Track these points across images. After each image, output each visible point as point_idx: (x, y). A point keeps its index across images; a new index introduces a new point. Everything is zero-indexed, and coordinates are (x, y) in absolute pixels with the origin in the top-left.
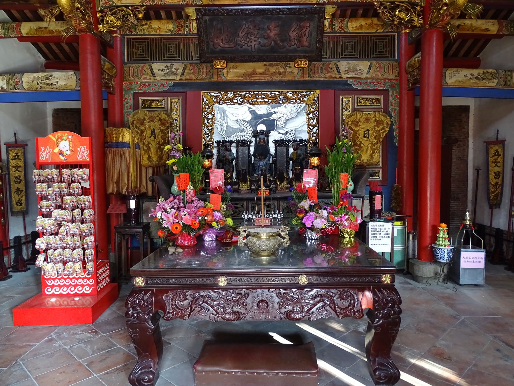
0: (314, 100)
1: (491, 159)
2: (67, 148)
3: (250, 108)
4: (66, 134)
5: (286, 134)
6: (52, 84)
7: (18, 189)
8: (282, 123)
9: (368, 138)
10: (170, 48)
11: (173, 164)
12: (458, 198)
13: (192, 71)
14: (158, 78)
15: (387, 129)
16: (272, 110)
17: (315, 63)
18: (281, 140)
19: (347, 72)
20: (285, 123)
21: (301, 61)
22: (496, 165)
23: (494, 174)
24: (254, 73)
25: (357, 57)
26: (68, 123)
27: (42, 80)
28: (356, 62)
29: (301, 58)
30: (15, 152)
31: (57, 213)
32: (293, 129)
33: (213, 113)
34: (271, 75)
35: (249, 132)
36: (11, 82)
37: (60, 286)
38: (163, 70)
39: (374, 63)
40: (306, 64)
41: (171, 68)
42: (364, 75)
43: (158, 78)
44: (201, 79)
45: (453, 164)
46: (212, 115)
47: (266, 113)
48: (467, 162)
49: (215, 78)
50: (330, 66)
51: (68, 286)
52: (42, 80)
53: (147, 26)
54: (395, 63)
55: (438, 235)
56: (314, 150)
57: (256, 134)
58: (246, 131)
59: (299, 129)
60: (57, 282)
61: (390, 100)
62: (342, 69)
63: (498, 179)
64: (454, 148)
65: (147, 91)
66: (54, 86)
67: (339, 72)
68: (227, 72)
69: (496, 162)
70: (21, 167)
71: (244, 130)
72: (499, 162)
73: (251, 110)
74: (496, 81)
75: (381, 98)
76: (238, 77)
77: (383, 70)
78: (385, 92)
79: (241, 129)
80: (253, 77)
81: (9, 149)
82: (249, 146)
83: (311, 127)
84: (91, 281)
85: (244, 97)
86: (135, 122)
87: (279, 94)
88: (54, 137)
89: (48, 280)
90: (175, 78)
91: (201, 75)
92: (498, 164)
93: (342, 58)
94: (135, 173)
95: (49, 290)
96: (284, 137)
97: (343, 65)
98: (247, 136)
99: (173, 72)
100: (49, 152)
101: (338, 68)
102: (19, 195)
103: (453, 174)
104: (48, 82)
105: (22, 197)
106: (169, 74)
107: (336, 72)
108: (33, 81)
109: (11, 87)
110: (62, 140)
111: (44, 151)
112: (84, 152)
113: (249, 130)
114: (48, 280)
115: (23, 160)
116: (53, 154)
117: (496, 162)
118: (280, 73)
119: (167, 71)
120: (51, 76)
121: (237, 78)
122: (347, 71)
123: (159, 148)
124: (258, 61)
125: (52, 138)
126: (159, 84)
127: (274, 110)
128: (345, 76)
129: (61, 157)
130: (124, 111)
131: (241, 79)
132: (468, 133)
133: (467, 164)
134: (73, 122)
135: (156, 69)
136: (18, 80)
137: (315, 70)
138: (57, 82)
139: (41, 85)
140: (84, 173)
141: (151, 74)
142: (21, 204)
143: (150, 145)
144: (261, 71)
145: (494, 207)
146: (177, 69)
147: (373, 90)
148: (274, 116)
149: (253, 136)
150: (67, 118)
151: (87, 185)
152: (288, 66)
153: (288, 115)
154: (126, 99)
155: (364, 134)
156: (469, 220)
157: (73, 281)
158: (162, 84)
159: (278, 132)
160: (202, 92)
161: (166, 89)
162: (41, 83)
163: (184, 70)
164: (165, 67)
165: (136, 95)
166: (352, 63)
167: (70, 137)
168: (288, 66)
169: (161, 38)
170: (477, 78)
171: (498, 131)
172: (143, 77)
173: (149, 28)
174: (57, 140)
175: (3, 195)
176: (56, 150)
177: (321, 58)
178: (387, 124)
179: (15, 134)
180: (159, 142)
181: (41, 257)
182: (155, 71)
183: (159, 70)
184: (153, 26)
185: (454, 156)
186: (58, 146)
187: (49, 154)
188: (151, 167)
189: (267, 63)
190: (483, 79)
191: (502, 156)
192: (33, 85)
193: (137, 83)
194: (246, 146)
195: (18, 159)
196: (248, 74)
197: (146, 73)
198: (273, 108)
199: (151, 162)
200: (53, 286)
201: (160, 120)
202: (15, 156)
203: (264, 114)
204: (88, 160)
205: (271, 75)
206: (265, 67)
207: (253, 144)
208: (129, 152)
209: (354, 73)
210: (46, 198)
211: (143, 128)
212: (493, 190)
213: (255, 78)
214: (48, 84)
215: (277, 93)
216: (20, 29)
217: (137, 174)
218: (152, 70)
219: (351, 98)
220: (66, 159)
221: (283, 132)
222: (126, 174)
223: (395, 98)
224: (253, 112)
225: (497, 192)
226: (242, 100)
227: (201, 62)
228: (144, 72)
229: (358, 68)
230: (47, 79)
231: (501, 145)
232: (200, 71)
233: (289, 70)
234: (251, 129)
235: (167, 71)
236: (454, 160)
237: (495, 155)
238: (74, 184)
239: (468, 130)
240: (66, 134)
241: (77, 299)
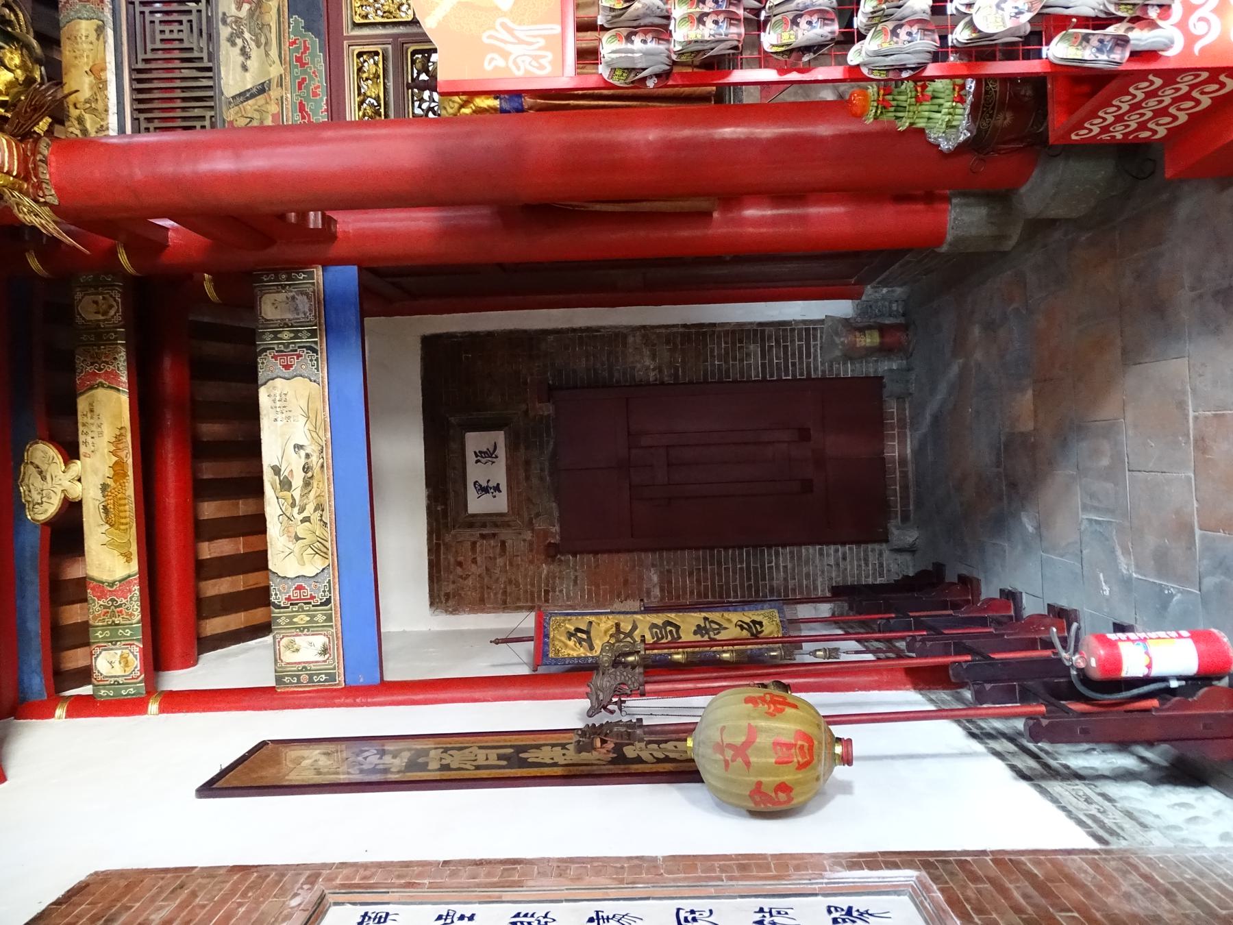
6: (306, 469)
7: (699, 630)
10: (167, 36)
14: (275, 70)
26: (474, 561)
27: (293, 505)
30: (563, 639)
36: (302, 619)
38: (244, 52)
41: (238, 20)
52: (293, 505)
53: (87, 116)
66: (314, 459)
70: (618, 625)
81: (551, 655)
100: (510, 31)
102: (721, 628)
104: (297, 481)
105: (729, 621)
106: (260, 28)
108: (297, 538)
109: (320, 618)
111: (505, 55)
115: (592, 618)
119: (247, 35)
120: (276, 470)
134: (474, 543)
135: (244, 80)
136: (294, 595)
138: (298, 447)
139: (310, 508)
141: (260, 99)
142: (760, 623)
150: (460, 564)
158: (299, 59)
161: (313, 41)
162: (302, 510)
164: (234, 44)
169: (132, 70)
173: (93, 111)
175: (724, 652)
179: (497, 642)
182: (249, 82)
183: (245, 68)
184: (86, 93)
187: (522, 31)
192: (310, 538)
195: (587, 632)
197: (256, 116)
202: (580, 641)
214: (307, 484)
216: (112, 584)
218: (245, 96)
230: (286, 485)
235: (247, 35)
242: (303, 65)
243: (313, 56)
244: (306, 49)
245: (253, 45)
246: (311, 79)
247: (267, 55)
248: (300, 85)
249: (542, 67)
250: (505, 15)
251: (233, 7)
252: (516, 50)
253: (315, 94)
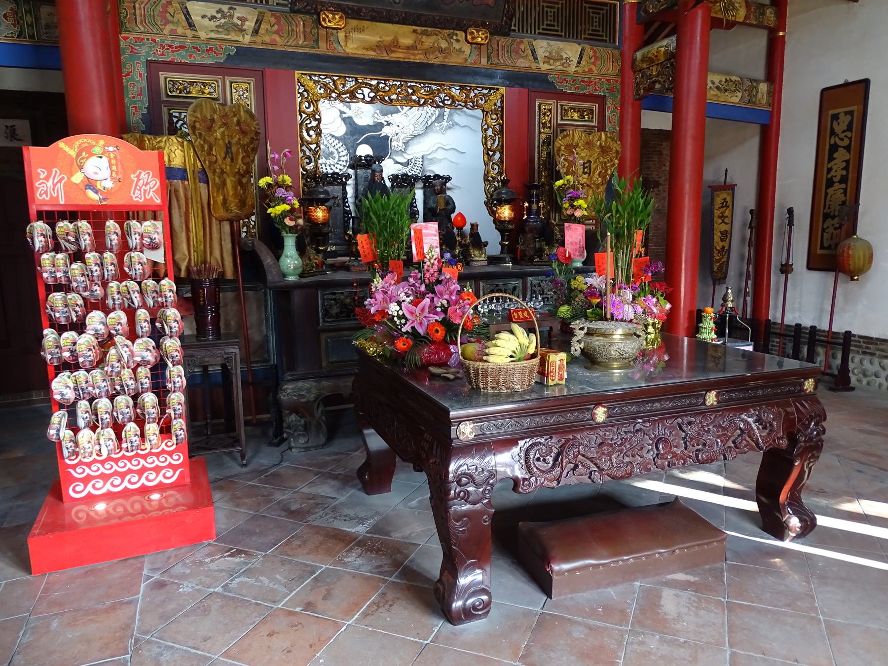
0: (495, 105)
2: (105, 173)
3: (342, 112)
4: (102, 142)
5: (407, 164)
8: (401, 144)
9: (589, 174)
11: (284, 214)
13: (276, 27)
15: (617, 161)
16: (383, 119)
17: (498, 38)
18: (403, 175)
19: (547, 60)
20: (406, 144)
21: (478, 32)
22: (723, 222)
23: (719, 235)
24: (394, 45)
25: (561, 36)
28: (560, 44)
29: (479, 26)
31: (95, 319)
32: (420, 155)
33: (317, 117)
34: (426, 52)
35: (342, 159)
37: (105, 477)
38: (213, 18)
39: (588, 48)
40: (486, 37)
41: (231, 16)
42: (573, 69)
43: (203, 35)
44: (296, 46)
46: (316, 120)
47: (371, 123)
49: (323, 49)
50: (522, 47)
51: (123, 475)
54: (616, 52)
55: (701, 325)
56: (504, 193)
57: (356, 163)
58: (337, 157)
59: (429, 157)
60: (97, 469)
61: (608, 114)
62: (541, 53)
65: (177, 59)
67: (535, 59)
68: (346, 36)
69: (723, 216)
71: (332, 153)
73: (344, 115)
74: (739, 94)
75: (595, 107)
76: (367, 49)
77: (599, 62)
78: (601, 100)
79: (327, 151)
80: (392, 52)
82: (344, 185)
83: (491, 153)
84: (176, 458)
85: (375, 89)
86: (197, 125)
87: (438, 90)
88: (71, 147)
89: (74, 467)
90: (240, 39)
91: (291, 38)
92: (726, 220)
93: (539, 33)
94: (201, 234)
95: (78, 489)
96: (405, 170)
97: (543, 46)
98: (338, 166)
99: (236, 25)
100: (60, 181)
101: (534, 52)
107: (531, 58)
110: (91, 155)
111: (47, 178)
112: (147, 184)
113: (342, 154)
114: (74, 467)
116: (69, 186)
118: (441, 51)
121: (365, 52)
122: (548, 58)
123: (240, 183)
124: (403, 22)
125: (67, 149)
126: (204, 47)
127: (386, 118)
128: (544, 67)
129: (91, 194)
130: (127, 101)
131: (372, 54)
135: (196, 15)
137: (498, 50)
140: (153, 229)
141: (185, 24)
143: (225, 175)
144: (407, 41)
146: (243, 20)
147: (584, 95)
148: (386, 131)
149: (351, 167)
151: (158, 256)
152: (455, 37)
153: (410, 130)
154: (128, 74)
155: (584, 169)
156: (732, 301)
157: (162, 459)
158: (211, 49)
159: (394, 160)
160: (297, 74)
161: (221, 59)
163: (259, 22)
164: (218, 12)
165: (153, 67)
166: (556, 45)
167: (111, 149)
168: (455, 37)
170: (718, 88)
171: (726, 171)
172: (169, 27)
174: (79, 154)
176: (77, 178)
177: (510, 30)
178: (617, 151)
180: (239, 169)
181: (59, 418)
182: (196, 18)
183: (204, 17)
186: (81, 168)
188: (228, 220)
189: (419, 29)
190: (726, 90)
193: (154, 40)
194: (339, 184)
196: (385, 46)
197: (175, 20)
198: (385, 114)
199: (227, 210)
200: (86, 480)
201: (239, 123)
203: (368, 126)
204: (158, 201)
205: (426, 52)
206: (414, 35)
207: (351, 182)
208: (185, 189)
209: (558, 63)
210: (65, 288)
211: (212, 139)
212: (718, 258)
213: (398, 56)
215: (434, 87)
217: (205, 235)
218: (187, 14)
219: (551, 104)
220: (104, 199)
221: (403, 161)
222: (184, 235)
223: (614, 111)
224: (349, 121)
226: (372, 95)
227: (293, 11)
228: (170, 18)
229: (565, 56)
231: (730, 191)
232: (293, 30)
233: (457, 46)
234: (345, 152)
235: (223, 21)
237: (722, 207)
238: (133, 254)
240: (102, 142)
241: (156, 496)
242: (208, 51)
243: (213, 58)
244: (217, 54)
245: (218, 23)
246: (199, 55)
247: (212, 31)
248: (196, 48)
249: (41, 195)
250: (69, 179)
251: (239, 15)
252: (50, 183)
253: (190, 56)
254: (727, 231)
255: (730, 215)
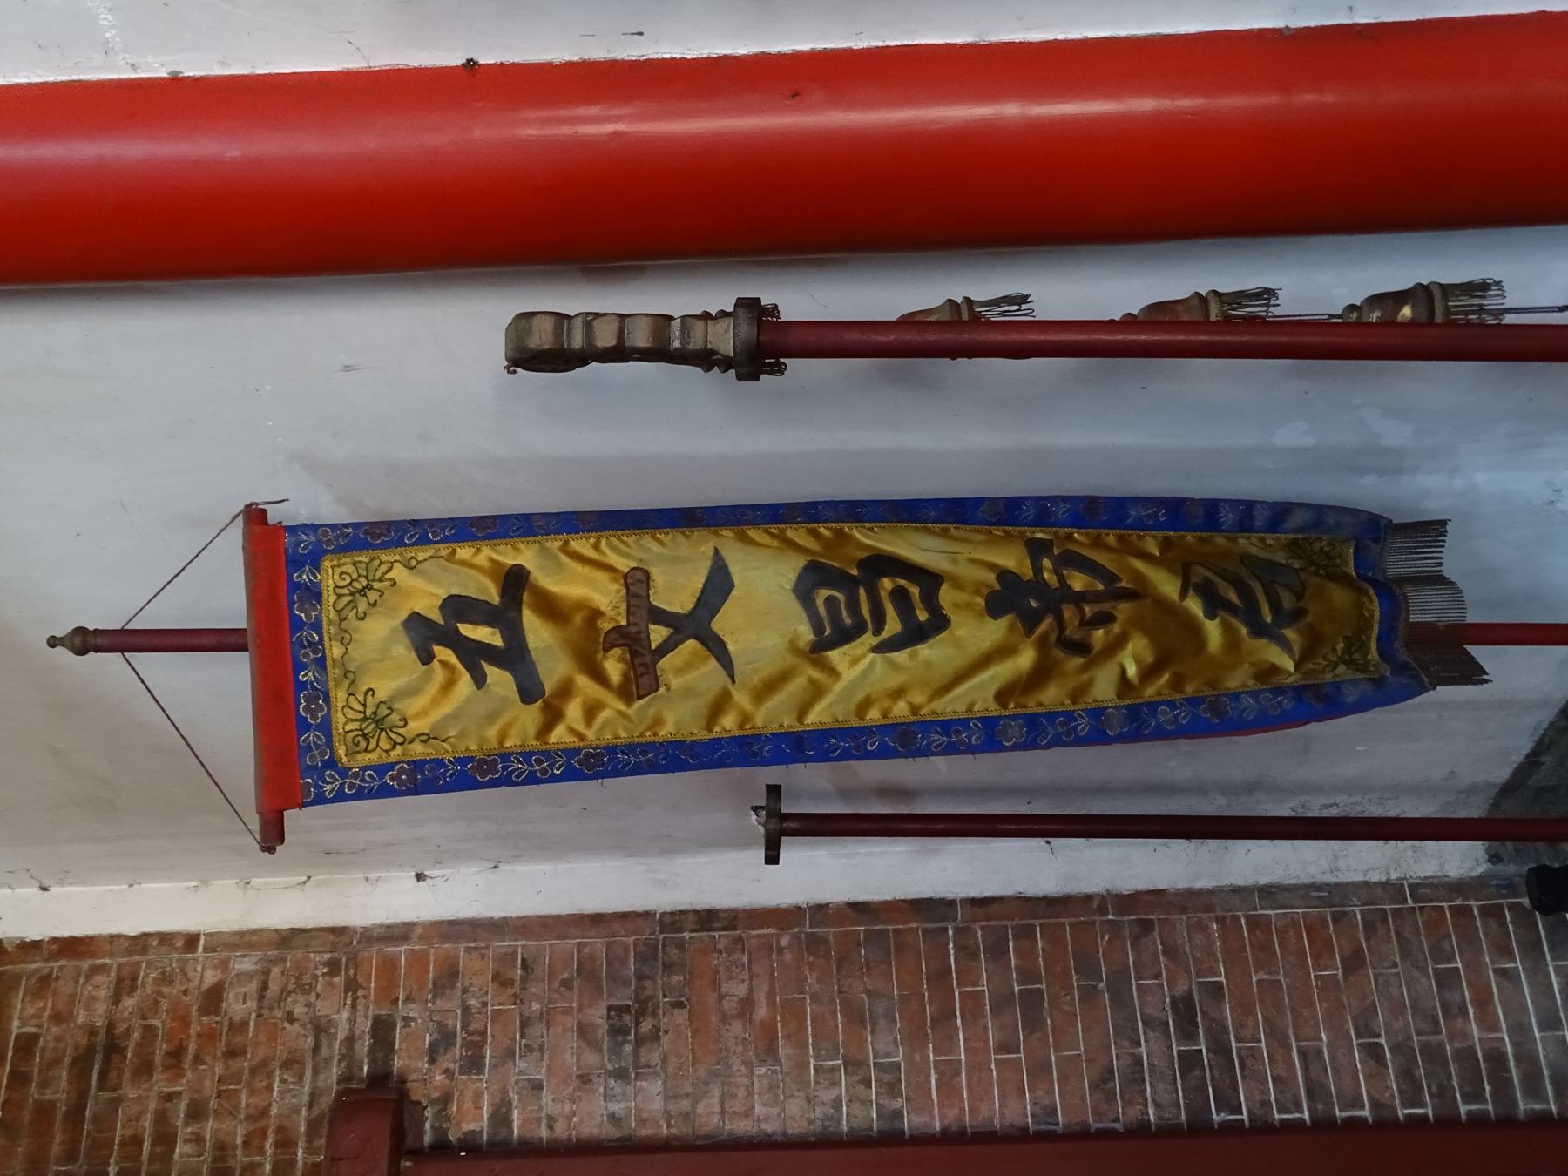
1: (596, 715)
12: (1184, 1010)
22: (696, 625)
45: (711, 1115)
48: (673, 921)
63: (930, 580)
64: (473, 1120)
69: (629, 639)
72: (636, 583)
92: (676, 590)
103: (855, 1107)
117: (634, 645)
132: (289, 939)
133: (707, 919)
145: (1424, 609)
171: (84, 641)
185: (591, 1115)
191: (523, 555)
225: (1167, 586)
231: (333, 575)
236: (645, 1105)
237: (514, 656)
239: (246, 940)
254: (814, 576)
255: (622, 553)
